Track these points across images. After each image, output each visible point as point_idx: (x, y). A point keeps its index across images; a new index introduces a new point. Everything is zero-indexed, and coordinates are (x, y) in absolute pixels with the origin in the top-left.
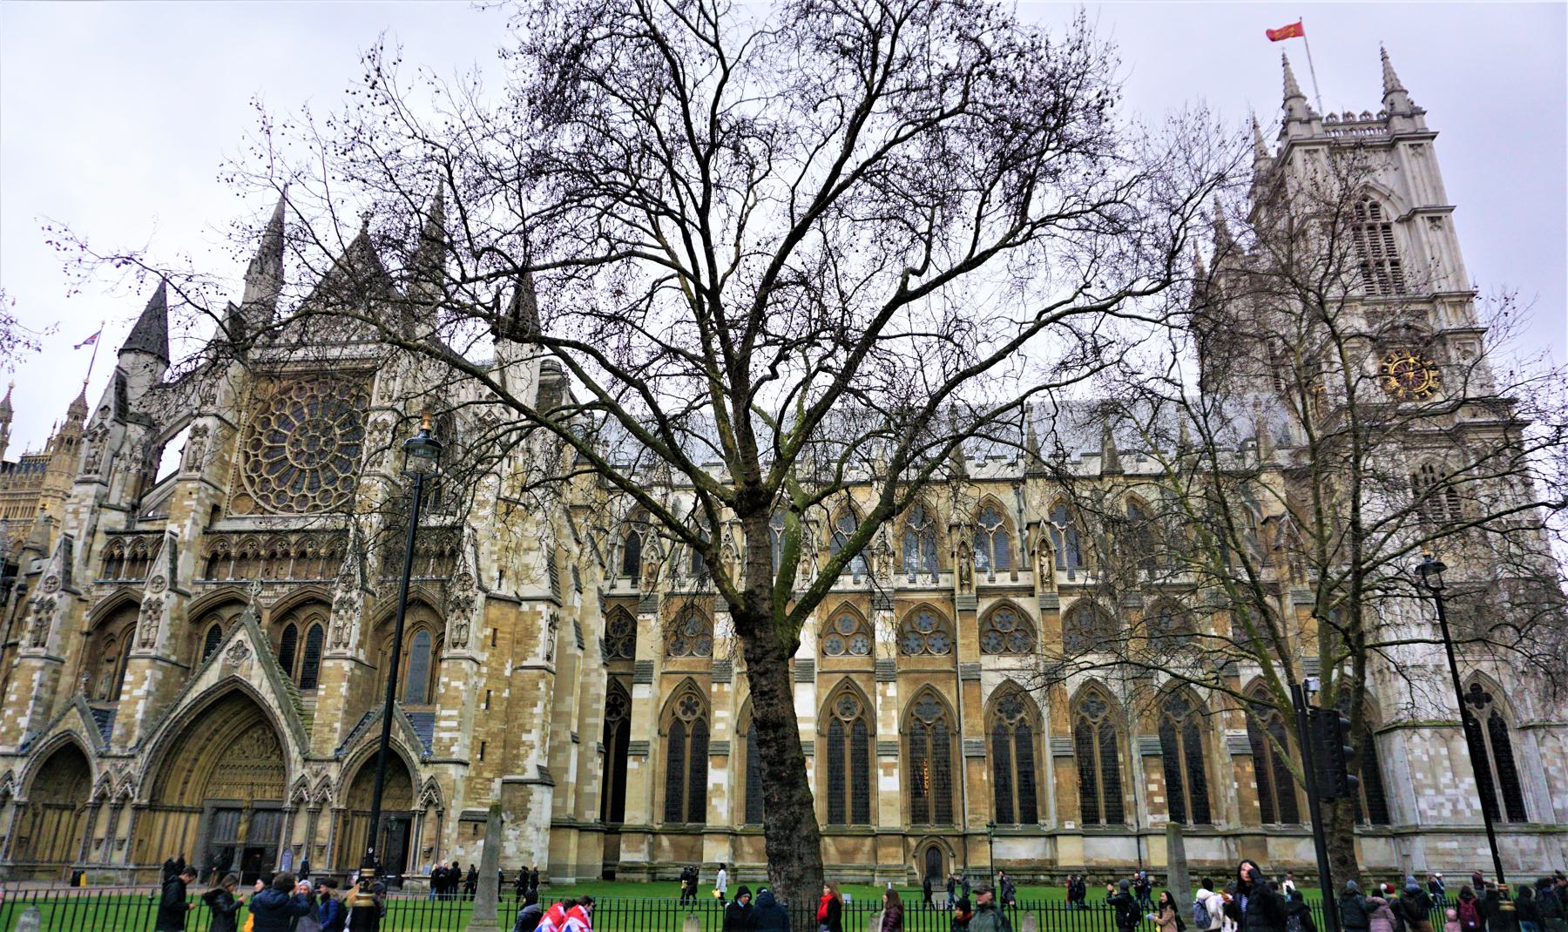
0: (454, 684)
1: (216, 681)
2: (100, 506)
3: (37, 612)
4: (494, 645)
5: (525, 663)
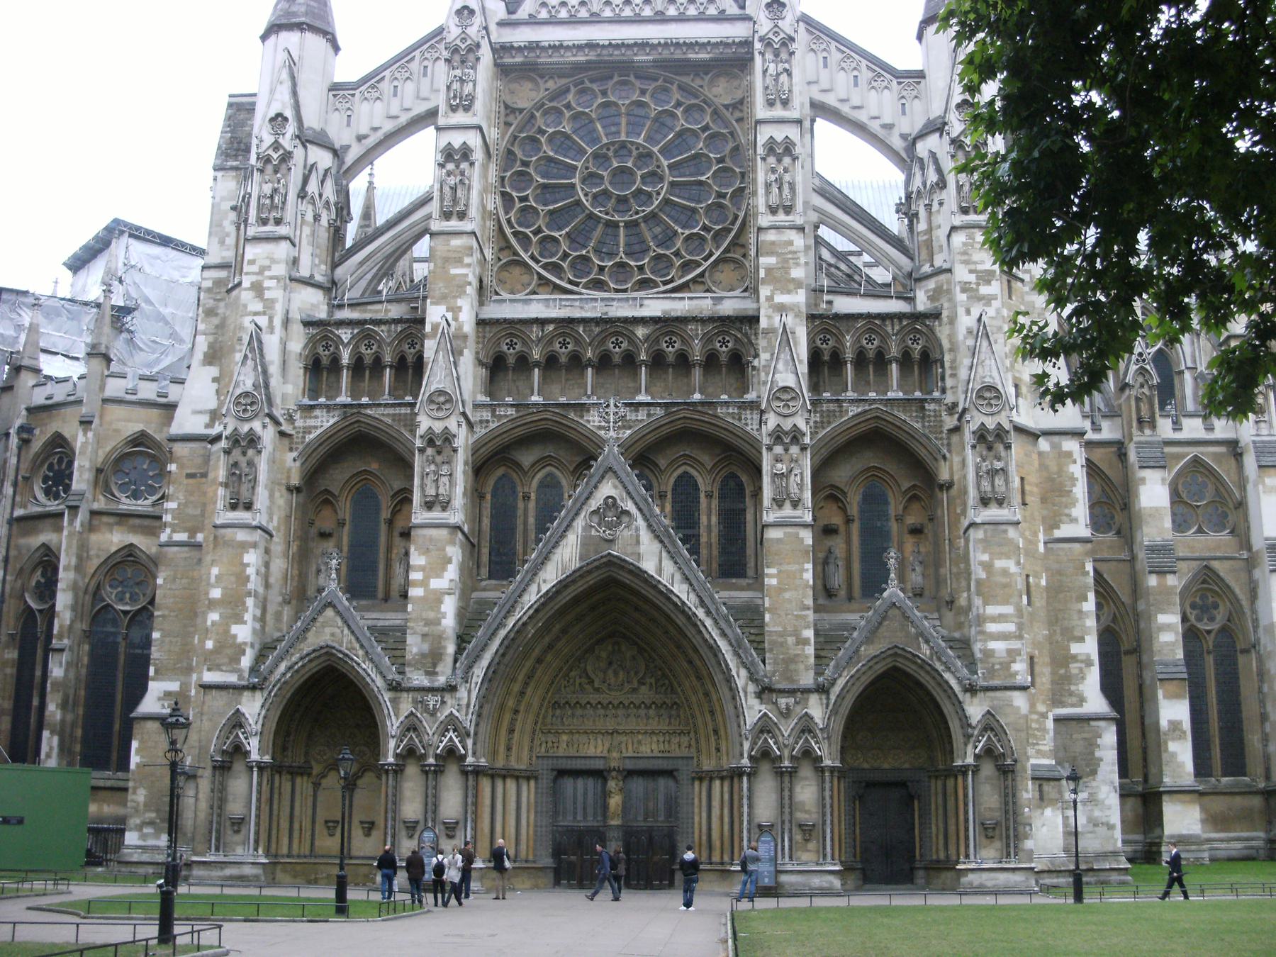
0: (999, 564)
1: (575, 564)
2: (291, 279)
3: (227, 452)
4: (1024, 504)
5: (1058, 534)
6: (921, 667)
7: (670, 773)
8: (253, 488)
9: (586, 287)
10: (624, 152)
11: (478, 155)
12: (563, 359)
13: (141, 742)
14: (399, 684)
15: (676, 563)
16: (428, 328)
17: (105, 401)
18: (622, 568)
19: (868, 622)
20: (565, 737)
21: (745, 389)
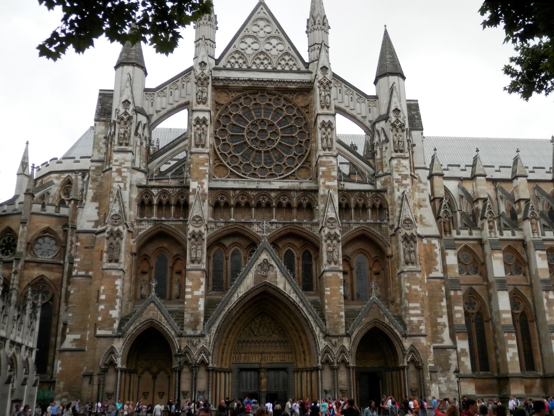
0: (414, 287)
1: (252, 285)
2: (133, 168)
3: (108, 238)
5: (431, 275)
6: (385, 327)
7: (284, 369)
8: (119, 253)
10: (263, 123)
11: (209, 122)
12: (243, 205)
13: (62, 361)
14: (181, 334)
15: (291, 285)
16: (191, 191)
17: (33, 214)
18: (270, 287)
19: (365, 309)
20: (243, 355)
21: (313, 218)
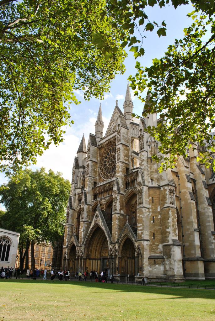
0: (140, 216)
2: (76, 188)
4: (153, 202)
5: (164, 206)
9: (108, 179)
